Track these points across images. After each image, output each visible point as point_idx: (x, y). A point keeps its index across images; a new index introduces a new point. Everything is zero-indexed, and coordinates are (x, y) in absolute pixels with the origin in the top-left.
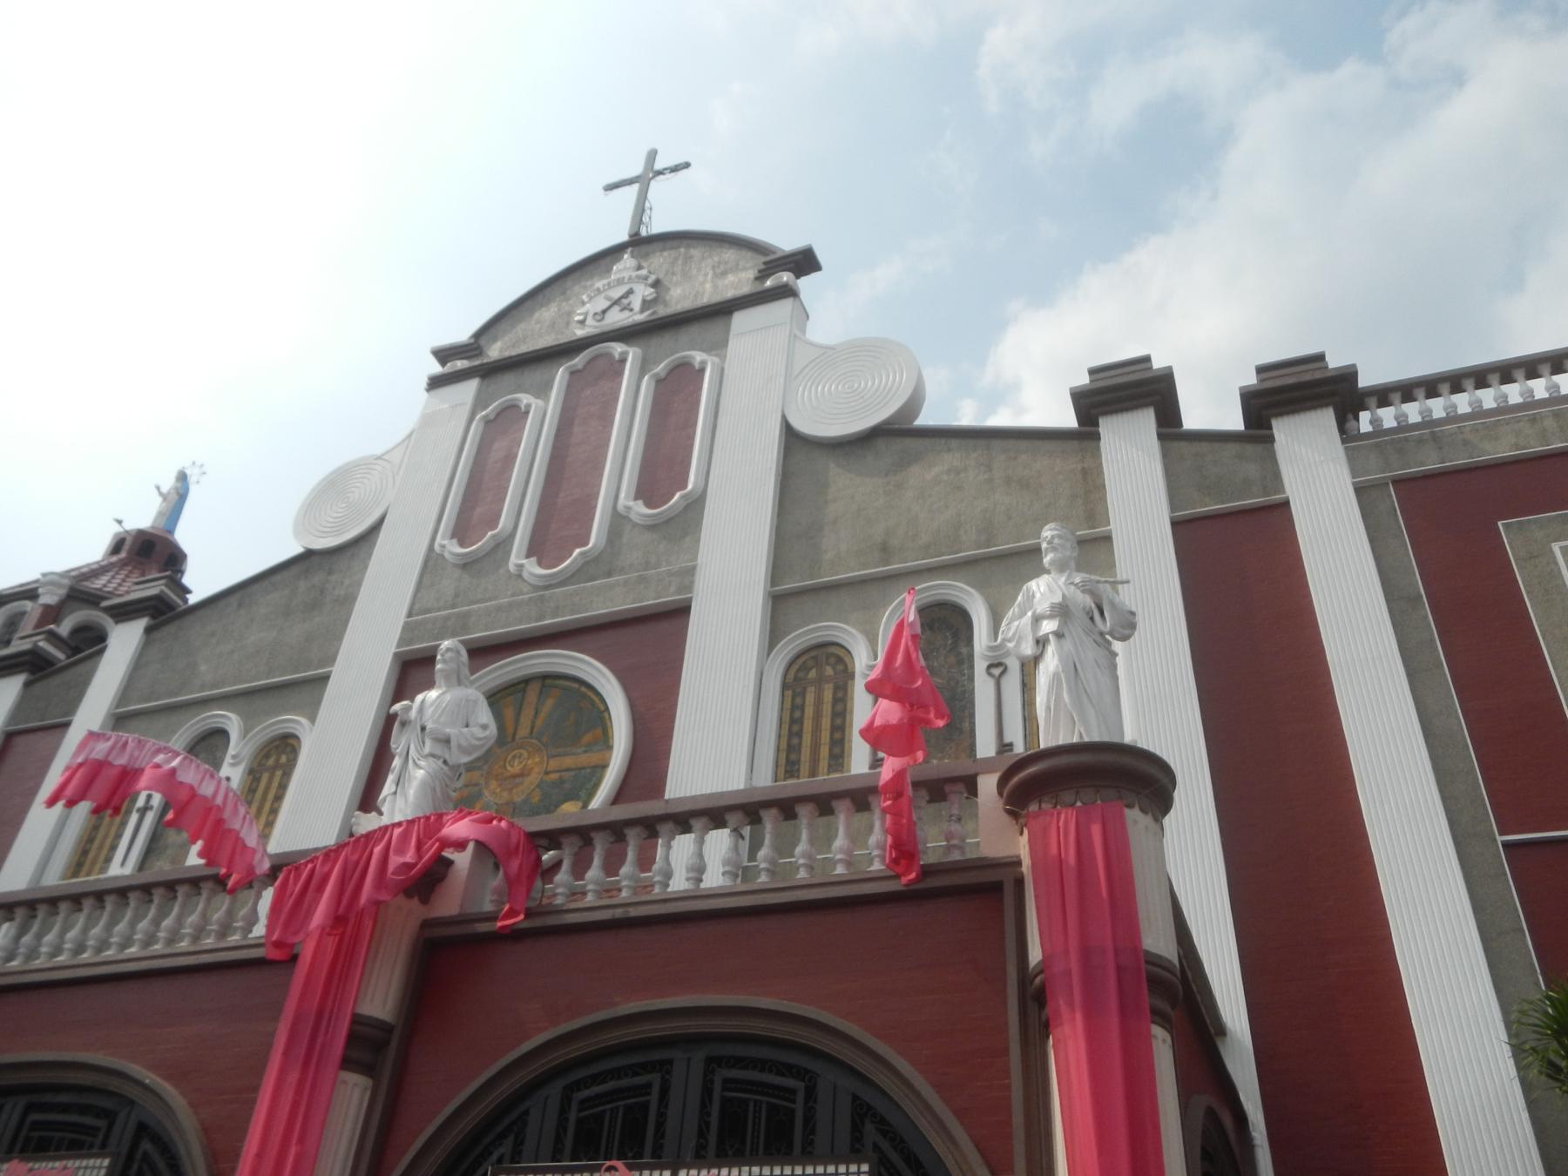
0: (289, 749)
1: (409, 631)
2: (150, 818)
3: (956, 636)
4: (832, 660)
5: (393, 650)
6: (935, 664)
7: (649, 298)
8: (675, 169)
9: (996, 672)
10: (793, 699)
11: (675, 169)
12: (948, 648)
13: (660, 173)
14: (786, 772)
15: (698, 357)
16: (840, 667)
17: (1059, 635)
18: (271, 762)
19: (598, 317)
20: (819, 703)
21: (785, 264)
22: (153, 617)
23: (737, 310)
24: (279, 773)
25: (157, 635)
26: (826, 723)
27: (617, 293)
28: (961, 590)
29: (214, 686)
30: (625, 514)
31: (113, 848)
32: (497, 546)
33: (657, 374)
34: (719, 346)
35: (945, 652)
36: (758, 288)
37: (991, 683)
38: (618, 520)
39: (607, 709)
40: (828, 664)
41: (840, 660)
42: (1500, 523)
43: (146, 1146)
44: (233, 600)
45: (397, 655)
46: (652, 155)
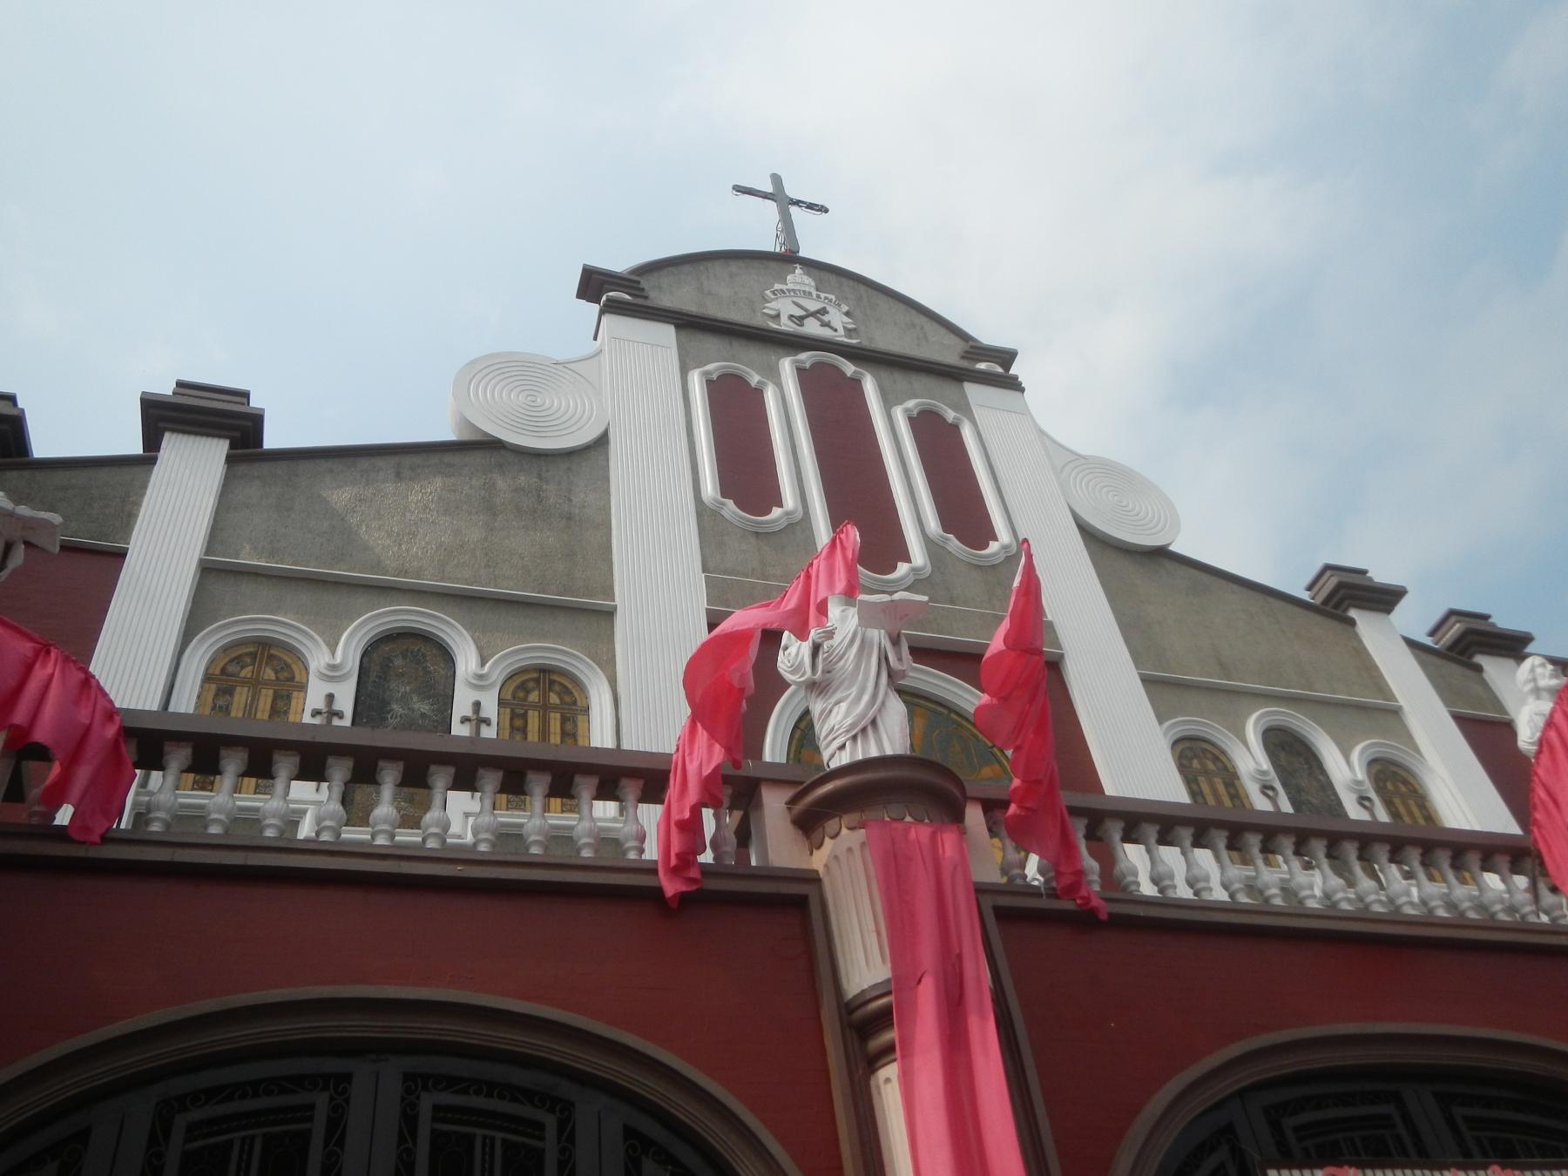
0: (557, 688)
4: (1209, 756)
7: (850, 326)
8: (811, 206)
11: (811, 206)
16: (1220, 765)
18: (534, 697)
21: (995, 357)
22: (232, 446)
23: (968, 381)
24: (555, 720)
25: (242, 468)
27: (813, 306)
28: (1304, 722)
29: (406, 574)
30: (942, 544)
32: (791, 527)
34: (964, 408)
36: (965, 364)
41: (1216, 759)
44: (380, 462)
45: (707, 609)
46: (776, 179)
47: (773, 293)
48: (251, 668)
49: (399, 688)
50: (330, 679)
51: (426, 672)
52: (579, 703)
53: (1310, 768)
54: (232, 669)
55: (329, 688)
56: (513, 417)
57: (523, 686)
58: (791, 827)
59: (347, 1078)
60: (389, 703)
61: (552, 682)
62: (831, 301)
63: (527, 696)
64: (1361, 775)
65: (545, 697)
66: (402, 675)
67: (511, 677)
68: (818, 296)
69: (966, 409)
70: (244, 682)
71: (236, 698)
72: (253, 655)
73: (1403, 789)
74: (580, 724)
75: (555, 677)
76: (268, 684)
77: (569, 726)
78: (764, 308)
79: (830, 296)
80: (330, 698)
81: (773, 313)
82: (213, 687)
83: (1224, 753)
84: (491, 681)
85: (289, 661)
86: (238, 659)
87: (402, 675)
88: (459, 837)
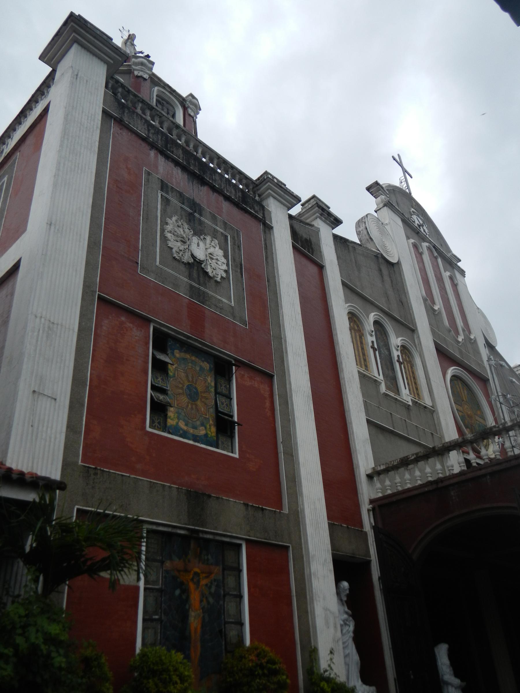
24: (409, 365)
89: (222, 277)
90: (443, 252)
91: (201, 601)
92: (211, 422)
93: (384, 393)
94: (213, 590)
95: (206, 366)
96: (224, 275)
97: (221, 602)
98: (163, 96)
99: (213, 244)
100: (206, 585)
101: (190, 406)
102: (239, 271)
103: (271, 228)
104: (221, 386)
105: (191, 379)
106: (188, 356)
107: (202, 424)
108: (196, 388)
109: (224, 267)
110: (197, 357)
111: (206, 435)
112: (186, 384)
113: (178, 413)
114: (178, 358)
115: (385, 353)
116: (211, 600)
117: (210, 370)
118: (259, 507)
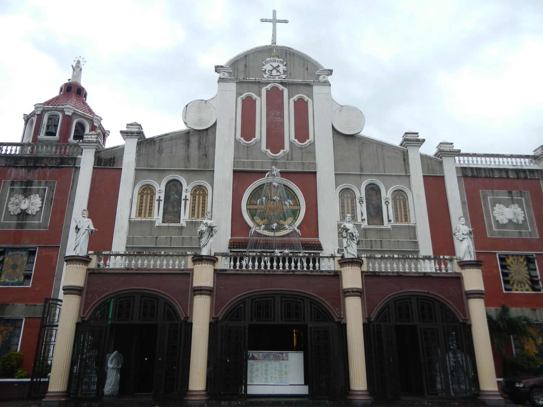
0: (202, 190)
1: (235, 163)
2: (162, 203)
3: (377, 192)
5: (232, 168)
6: (373, 198)
7: (285, 70)
9: (387, 203)
10: (341, 201)
12: (375, 195)
13: (280, 21)
14: (342, 218)
15: (306, 98)
16: (352, 195)
17: (467, 238)
18: (197, 192)
19: (270, 72)
20: (347, 203)
24: (201, 197)
26: (350, 208)
27: (275, 65)
31: (151, 210)
32: (256, 143)
33: (294, 100)
35: (374, 196)
37: (386, 206)
38: (291, 143)
39: (296, 195)
40: (349, 194)
42: (480, 191)
43: (313, 306)
45: (233, 169)
46: (274, 12)
47: (266, 63)
48: (146, 191)
49: (172, 193)
50: (160, 193)
51: (177, 188)
52: (206, 193)
53: (377, 194)
54: (143, 191)
55: (159, 195)
56: (195, 121)
57: (195, 190)
58: (192, 262)
59: (135, 296)
60: (170, 196)
61: (201, 189)
62: (281, 61)
63: (196, 193)
64: (389, 195)
65: (200, 192)
66: (172, 190)
67: (193, 188)
68: (278, 60)
69: (311, 96)
70: (145, 194)
71: (144, 197)
72: (146, 188)
73: (401, 197)
74: (206, 198)
75: (202, 187)
76: (149, 194)
77: (204, 199)
78: (262, 68)
79: (282, 60)
80: (160, 197)
81: (264, 70)
82: (140, 195)
83: (354, 192)
84: (189, 190)
85: (153, 189)
86: (144, 189)
87: (172, 190)
88: (182, 224)
89: (37, 211)
90: (293, 81)
91: (2, 338)
92: (22, 275)
93: (157, 226)
94: (8, 335)
95: (24, 253)
96: (38, 210)
97: (11, 339)
98: (52, 114)
99: (35, 198)
100: (5, 333)
101: (12, 272)
102: (50, 203)
103: (79, 168)
104: (30, 259)
105: (15, 261)
106: (15, 252)
107: (17, 278)
108: (17, 265)
109: (40, 205)
110: (20, 251)
111: (18, 281)
112: (12, 263)
113: (6, 276)
114: (10, 255)
115: (175, 197)
116: (7, 338)
117: (26, 254)
118: (33, 305)
